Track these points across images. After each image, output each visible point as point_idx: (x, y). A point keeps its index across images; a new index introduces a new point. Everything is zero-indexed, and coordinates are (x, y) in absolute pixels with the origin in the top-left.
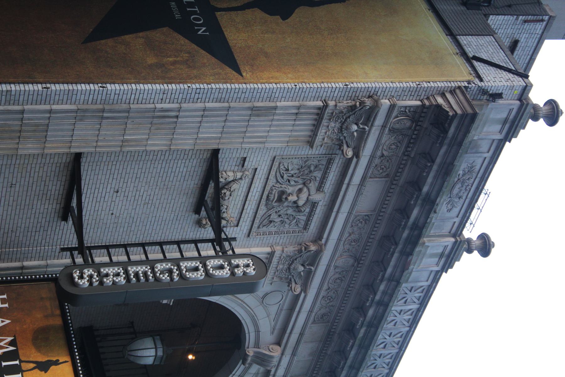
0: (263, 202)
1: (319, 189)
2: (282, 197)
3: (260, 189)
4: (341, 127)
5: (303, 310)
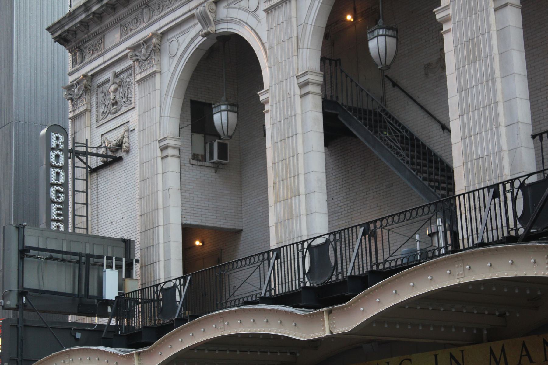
0: (119, 113)
1: (108, 81)
2: (115, 104)
3: (114, 122)
4: (79, 98)
5: (173, 18)
